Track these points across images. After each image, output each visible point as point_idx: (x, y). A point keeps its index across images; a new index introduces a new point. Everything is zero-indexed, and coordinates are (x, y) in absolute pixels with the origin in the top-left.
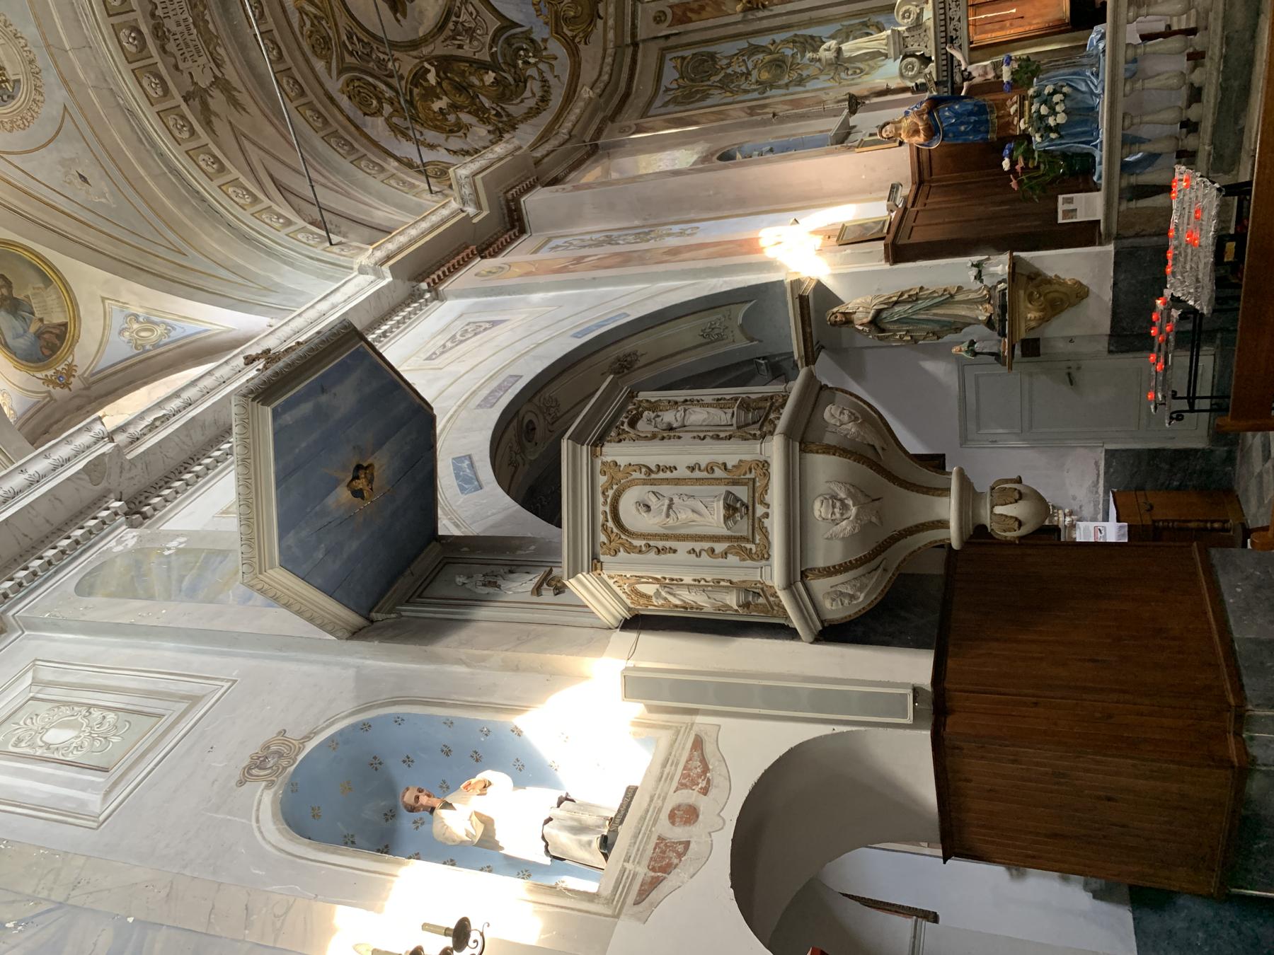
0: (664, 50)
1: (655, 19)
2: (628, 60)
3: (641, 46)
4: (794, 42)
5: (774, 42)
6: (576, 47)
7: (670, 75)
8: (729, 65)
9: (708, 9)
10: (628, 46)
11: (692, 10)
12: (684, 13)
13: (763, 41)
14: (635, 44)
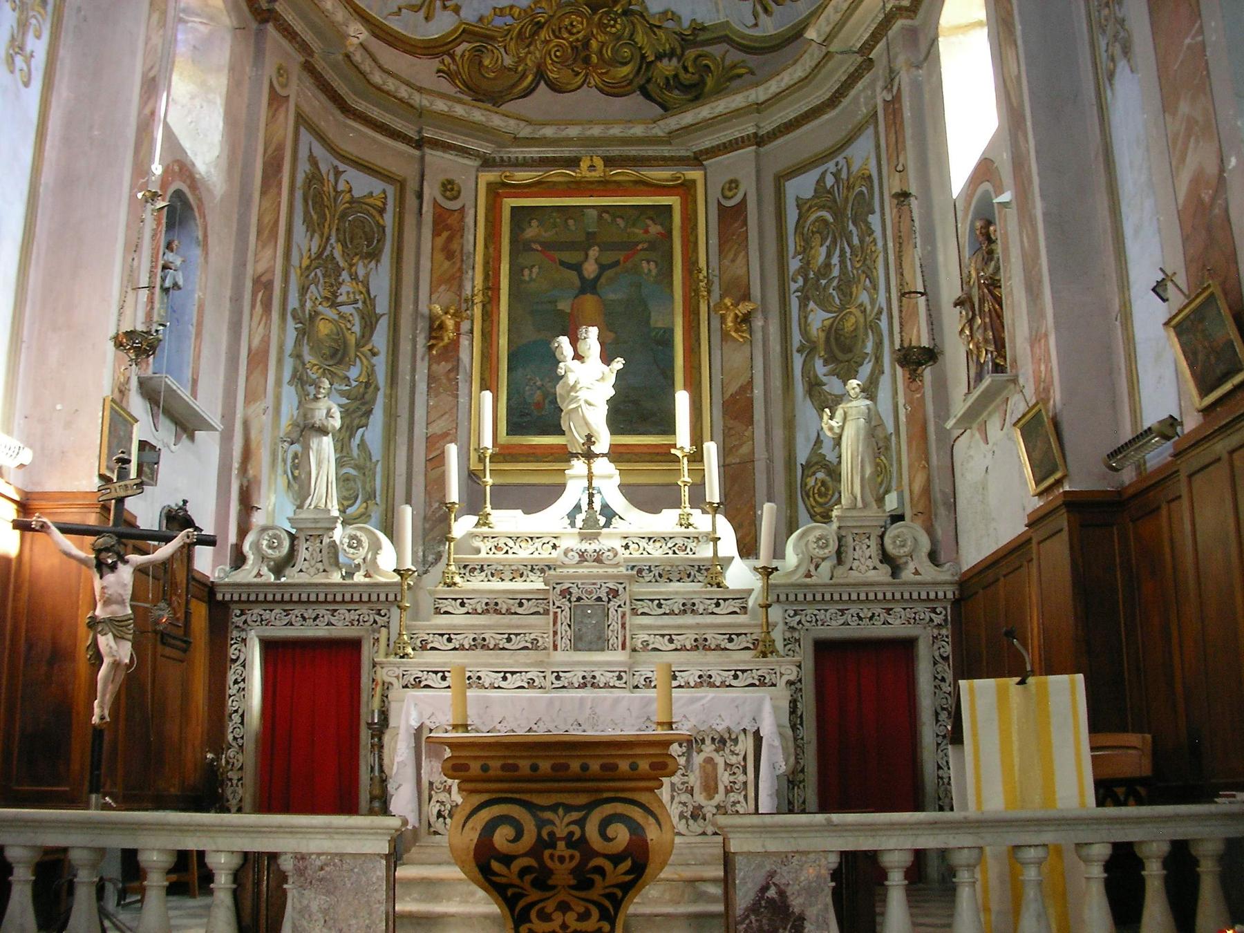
0: (401, 185)
1: (450, 182)
2: (398, 124)
3: (417, 153)
4: (367, 385)
5: (374, 354)
6: (435, 56)
7: (361, 185)
8: (354, 277)
9: (447, 264)
10: (420, 132)
11: (450, 240)
12: (448, 227)
13: (380, 339)
14: (420, 144)
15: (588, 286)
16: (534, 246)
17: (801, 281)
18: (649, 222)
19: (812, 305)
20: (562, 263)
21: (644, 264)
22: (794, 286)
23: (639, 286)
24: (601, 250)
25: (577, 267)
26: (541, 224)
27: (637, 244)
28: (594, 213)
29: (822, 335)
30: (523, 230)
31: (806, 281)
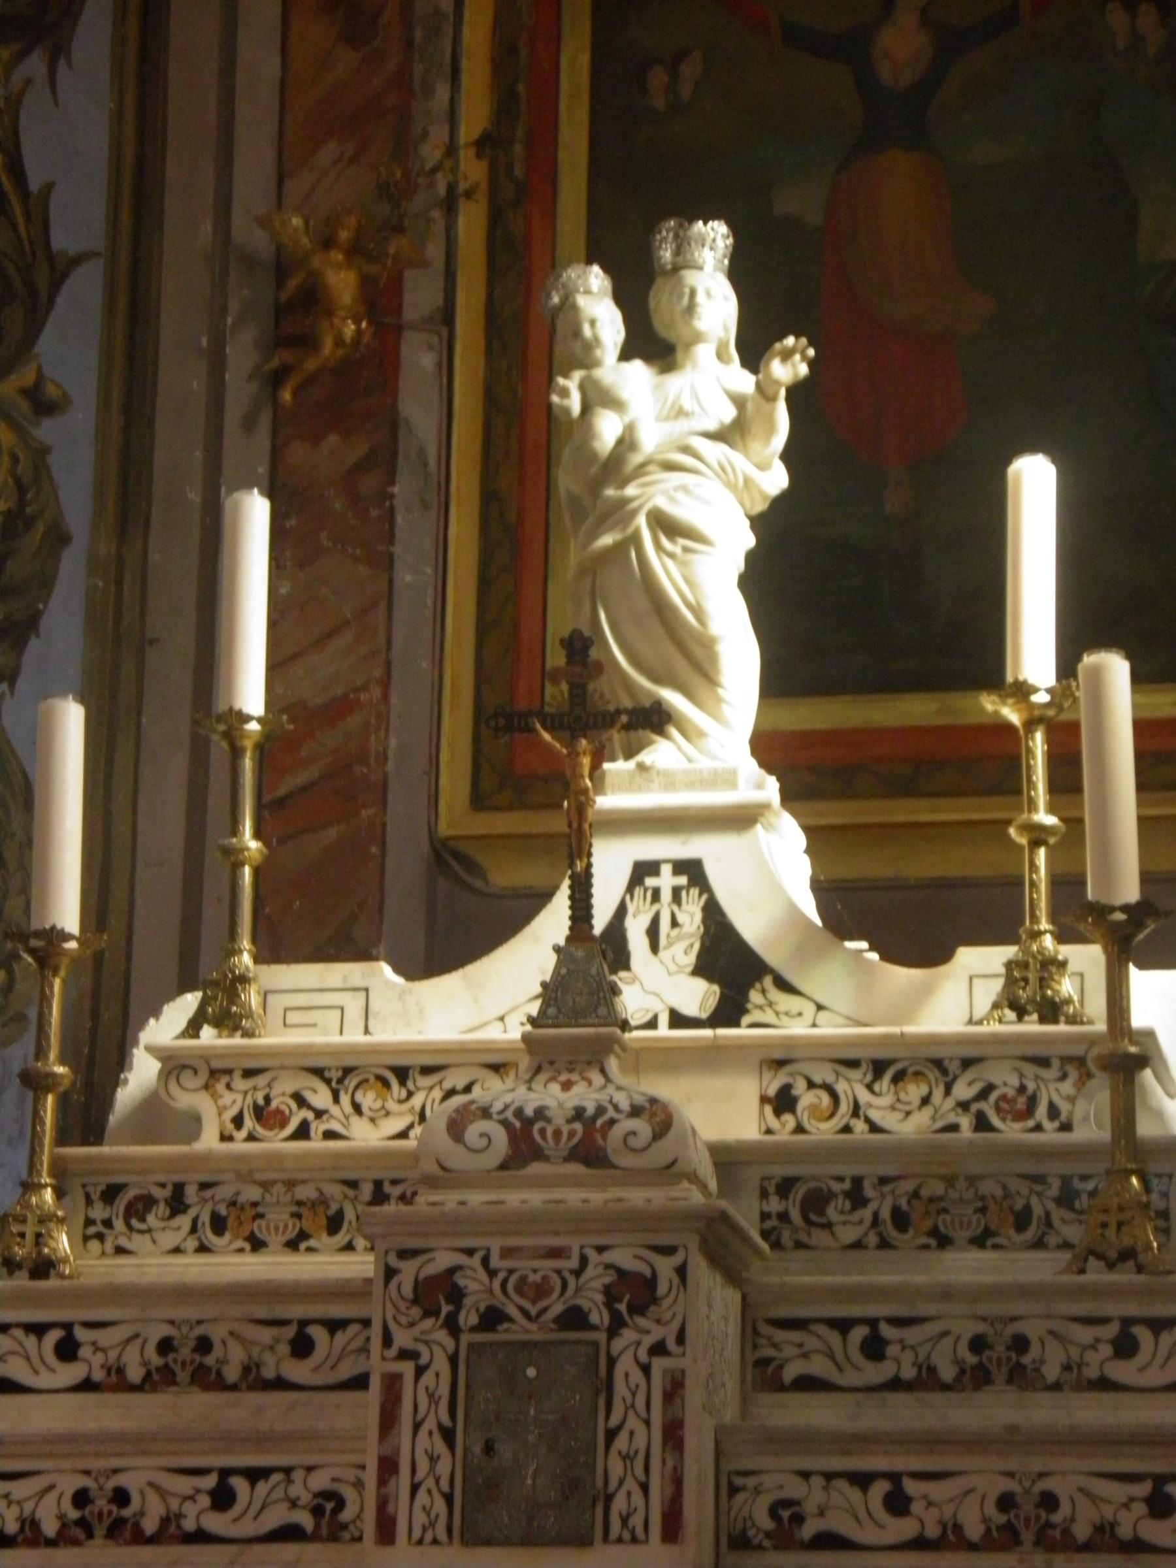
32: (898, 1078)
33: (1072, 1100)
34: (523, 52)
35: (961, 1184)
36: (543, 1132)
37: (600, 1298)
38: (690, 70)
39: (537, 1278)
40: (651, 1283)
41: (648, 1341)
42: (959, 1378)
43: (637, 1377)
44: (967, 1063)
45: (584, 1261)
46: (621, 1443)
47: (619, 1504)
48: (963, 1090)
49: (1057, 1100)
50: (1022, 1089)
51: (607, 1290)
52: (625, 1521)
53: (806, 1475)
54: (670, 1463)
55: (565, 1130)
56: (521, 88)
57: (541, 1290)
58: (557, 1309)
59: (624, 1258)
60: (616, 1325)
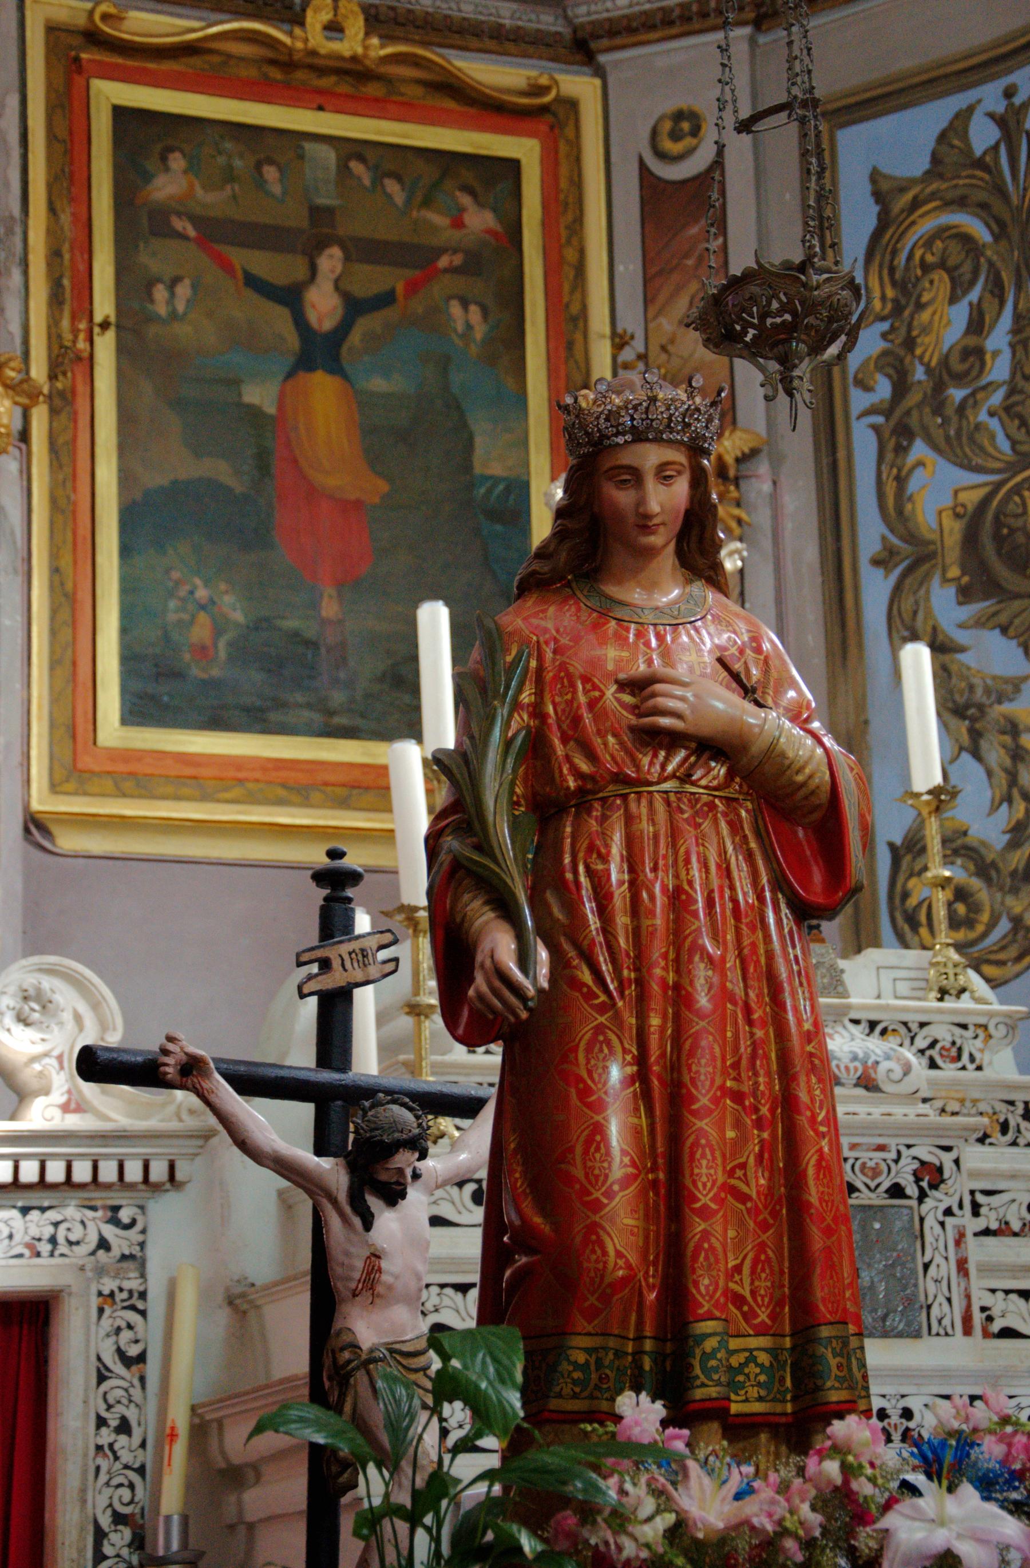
15: (319, 352)
16: (179, 224)
17: (883, 389)
18: (466, 200)
19: (919, 450)
20: (253, 282)
21: (455, 309)
22: (859, 400)
23: (444, 363)
24: (347, 258)
25: (291, 297)
26: (193, 167)
27: (441, 251)
28: (329, 156)
29: (954, 530)
30: (147, 177)
31: (901, 387)
32: (884, 1032)
33: (982, 1051)
34: (67, 257)
35: (968, 1104)
36: (838, 1066)
37: (912, 1178)
38: (183, 290)
39: (871, 1164)
40: (940, 1170)
41: (943, 1207)
42: (1022, 1229)
43: (938, 1229)
44: (922, 1025)
45: (899, 1153)
46: (932, 1271)
47: (935, 1312)
48: (921, 1043)
49: (974, 1052)
50: (954, 1043)
51: (915, 1173)
52: (940, 1322)
53: (993, 1291)
54: (963, 1285)
55: (851, 1066)
56: (66, 282)
57: (876, 1172)
58: (886, 1185)
59: (925, 1153)
60: (922, 1196)
